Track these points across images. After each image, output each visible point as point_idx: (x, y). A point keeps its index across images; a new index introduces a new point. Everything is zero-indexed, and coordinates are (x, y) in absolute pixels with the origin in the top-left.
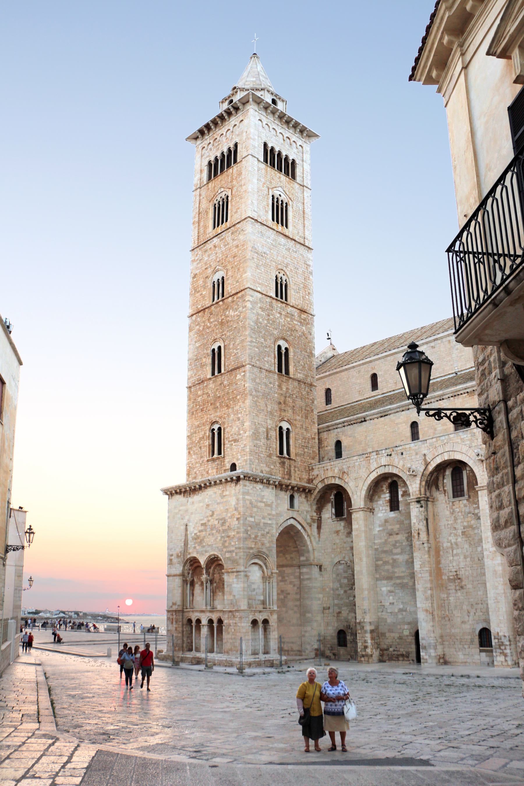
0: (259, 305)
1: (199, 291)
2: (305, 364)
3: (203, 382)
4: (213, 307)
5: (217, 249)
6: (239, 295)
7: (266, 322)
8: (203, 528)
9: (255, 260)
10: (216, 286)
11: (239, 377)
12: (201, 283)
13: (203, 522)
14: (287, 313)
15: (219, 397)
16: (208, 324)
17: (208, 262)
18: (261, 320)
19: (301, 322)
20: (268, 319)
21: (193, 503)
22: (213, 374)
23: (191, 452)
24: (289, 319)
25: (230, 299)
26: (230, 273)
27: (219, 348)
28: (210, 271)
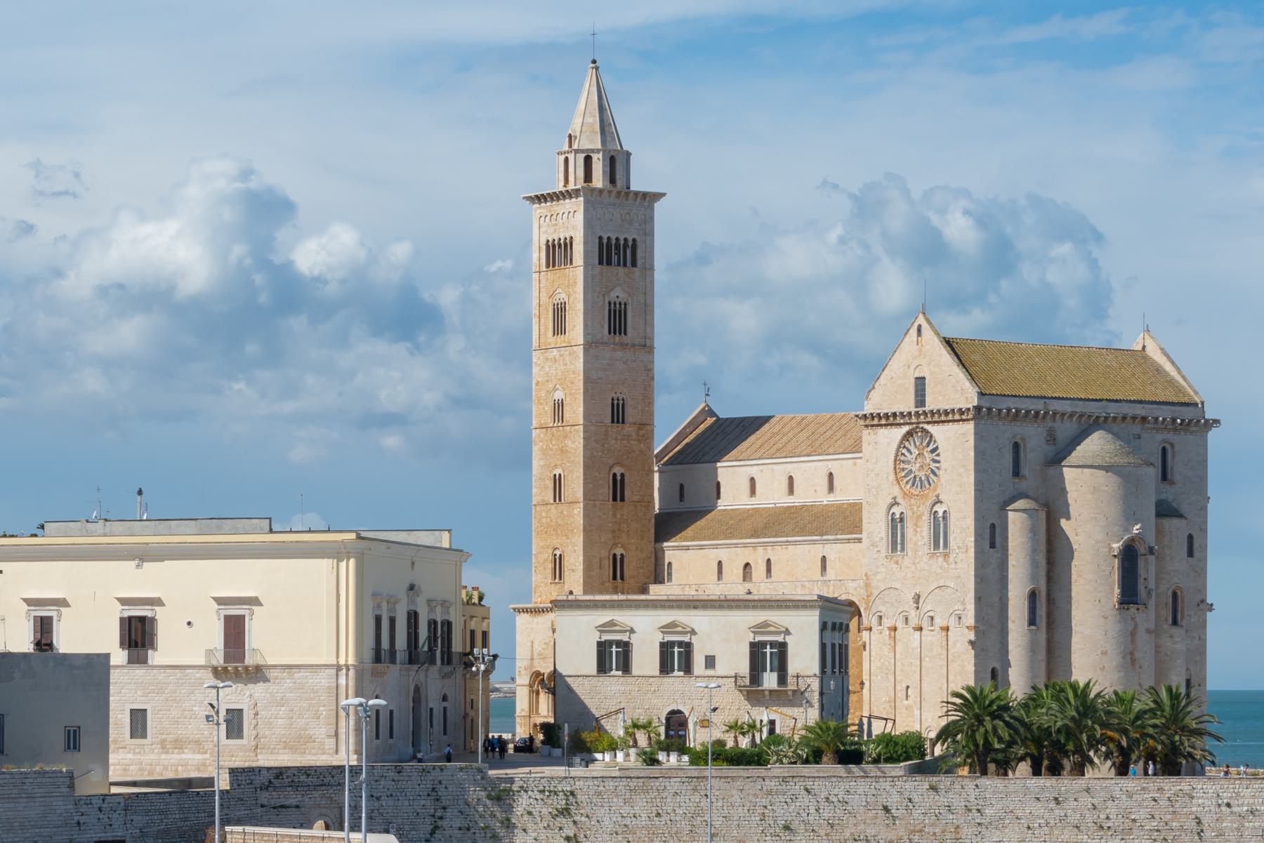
0: (593, 439)
1: (541, 404)
2: (642, 484)
3: (546, 504)
4: (554, 429)
5: (557, 363)
6: (576, 427)
7: (600, 454)
8: (545, 647)
9: (590, 390)
10: (557, 406)
11: (575, 512)
12: (543, 395)
13: (546, 641)
14: (624, 435)
15: (560, 525)
16: (551, 446)
17: (550, 375)
18: (595, 454)
19: (639, 440)
20: (603, 450)
21: (538, 623)
22: (555, 500)
23: (537, 571)
24: (625, 442)
25: (568, 428)
26: (568, 399)
27: (560, 475)
28: (551, 386)
